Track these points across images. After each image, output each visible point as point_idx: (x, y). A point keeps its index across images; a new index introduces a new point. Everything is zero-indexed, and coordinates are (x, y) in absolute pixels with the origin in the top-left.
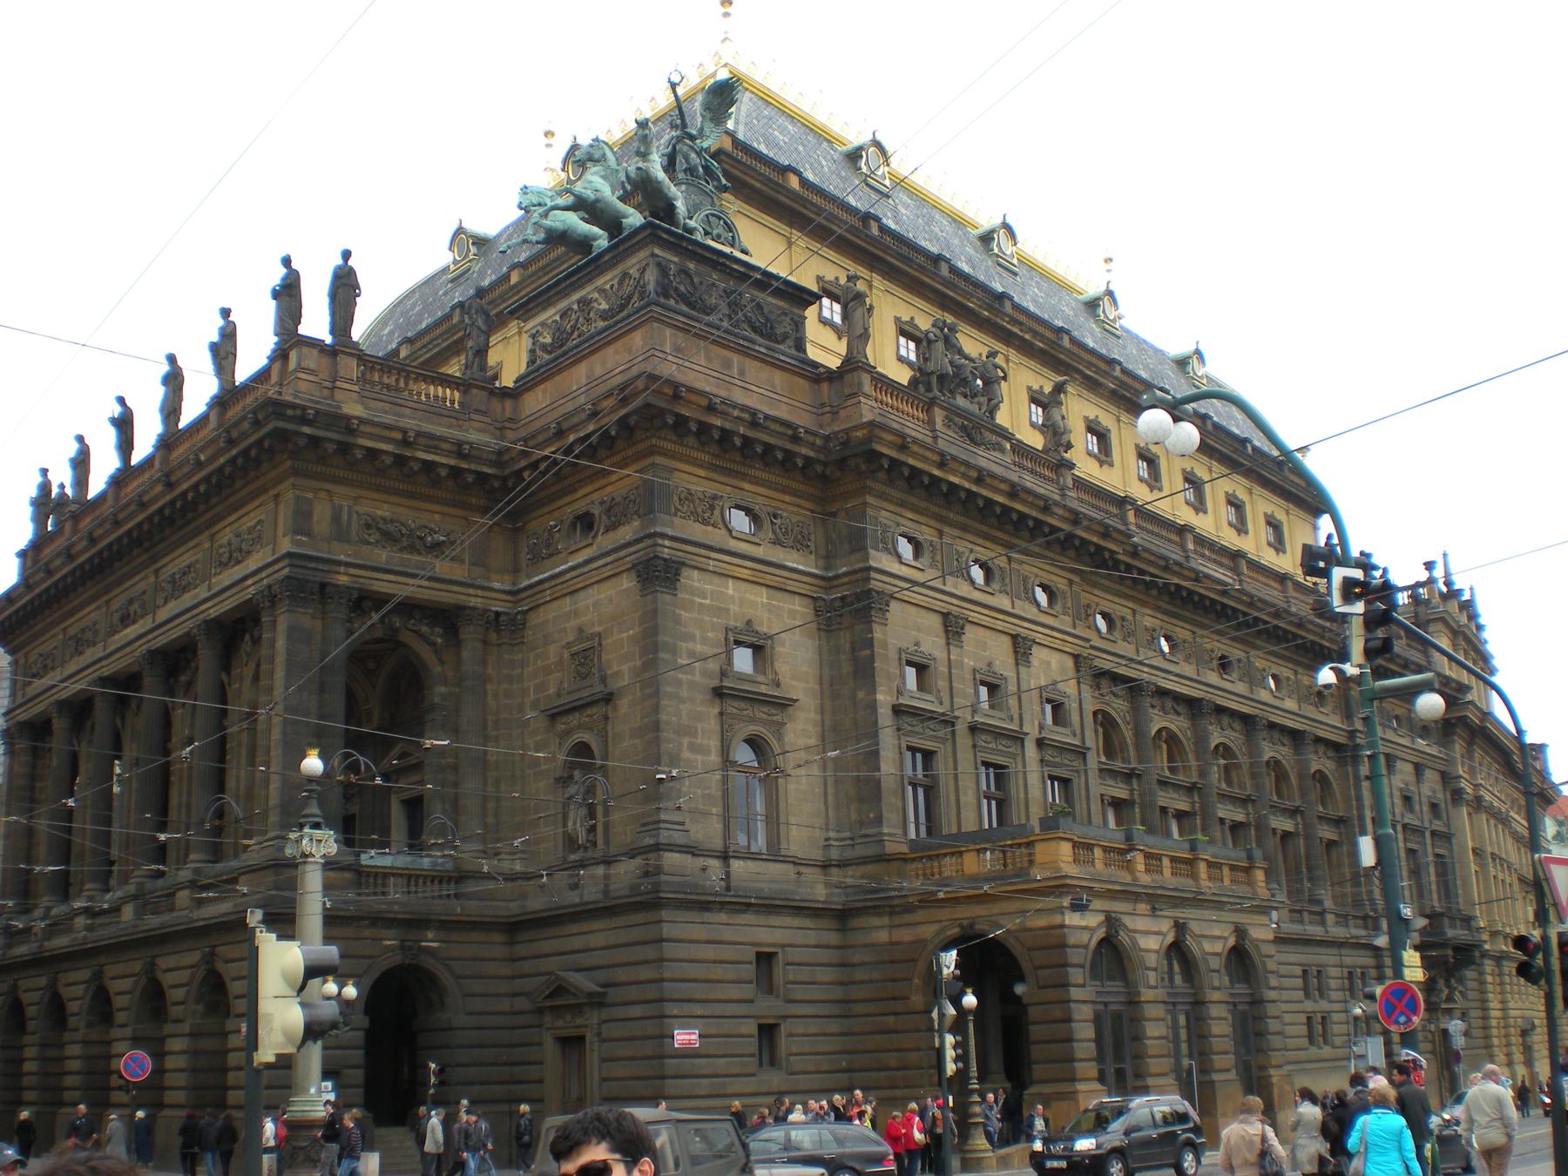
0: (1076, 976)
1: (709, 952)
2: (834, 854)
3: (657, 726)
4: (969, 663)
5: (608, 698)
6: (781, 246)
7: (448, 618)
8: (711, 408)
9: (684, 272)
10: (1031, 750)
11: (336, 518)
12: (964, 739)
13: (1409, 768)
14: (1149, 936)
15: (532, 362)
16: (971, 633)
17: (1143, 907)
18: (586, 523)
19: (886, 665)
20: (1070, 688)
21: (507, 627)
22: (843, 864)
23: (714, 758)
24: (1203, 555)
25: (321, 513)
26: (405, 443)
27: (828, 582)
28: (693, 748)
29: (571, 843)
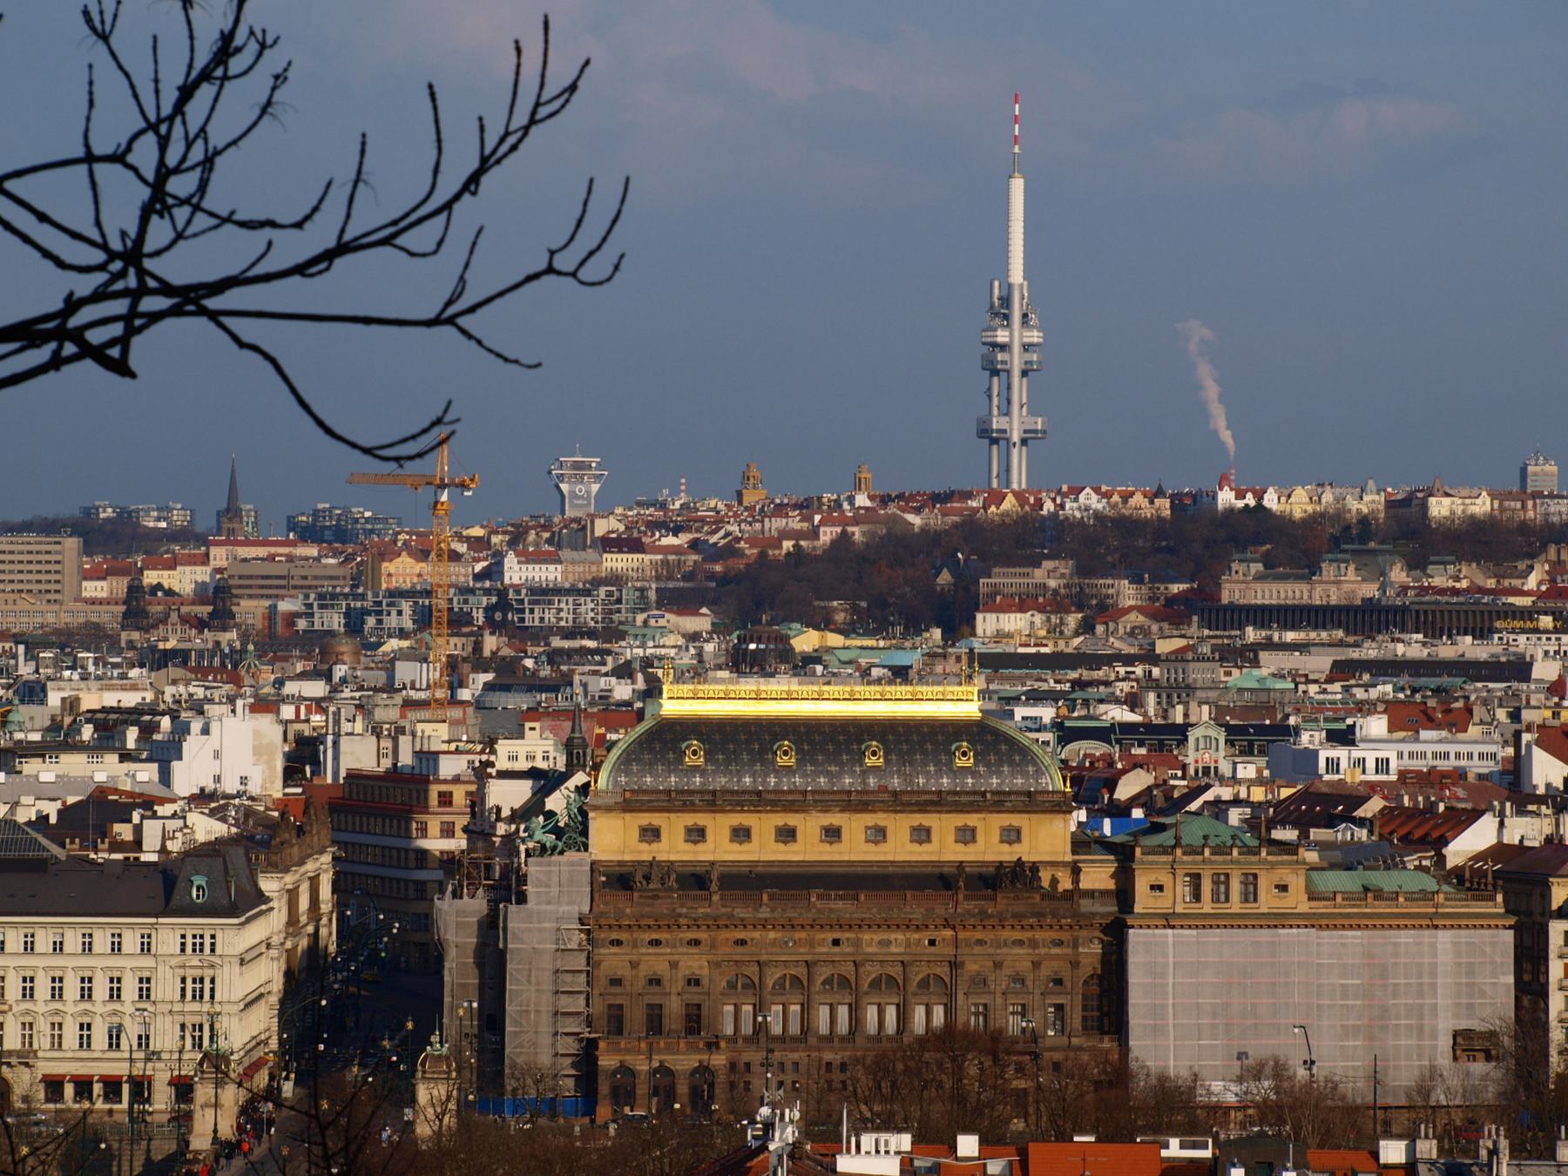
4: (642, 974)
6: (620, 822)
10: (674, 997)
14: (642, 1066)
20: (705, 972)
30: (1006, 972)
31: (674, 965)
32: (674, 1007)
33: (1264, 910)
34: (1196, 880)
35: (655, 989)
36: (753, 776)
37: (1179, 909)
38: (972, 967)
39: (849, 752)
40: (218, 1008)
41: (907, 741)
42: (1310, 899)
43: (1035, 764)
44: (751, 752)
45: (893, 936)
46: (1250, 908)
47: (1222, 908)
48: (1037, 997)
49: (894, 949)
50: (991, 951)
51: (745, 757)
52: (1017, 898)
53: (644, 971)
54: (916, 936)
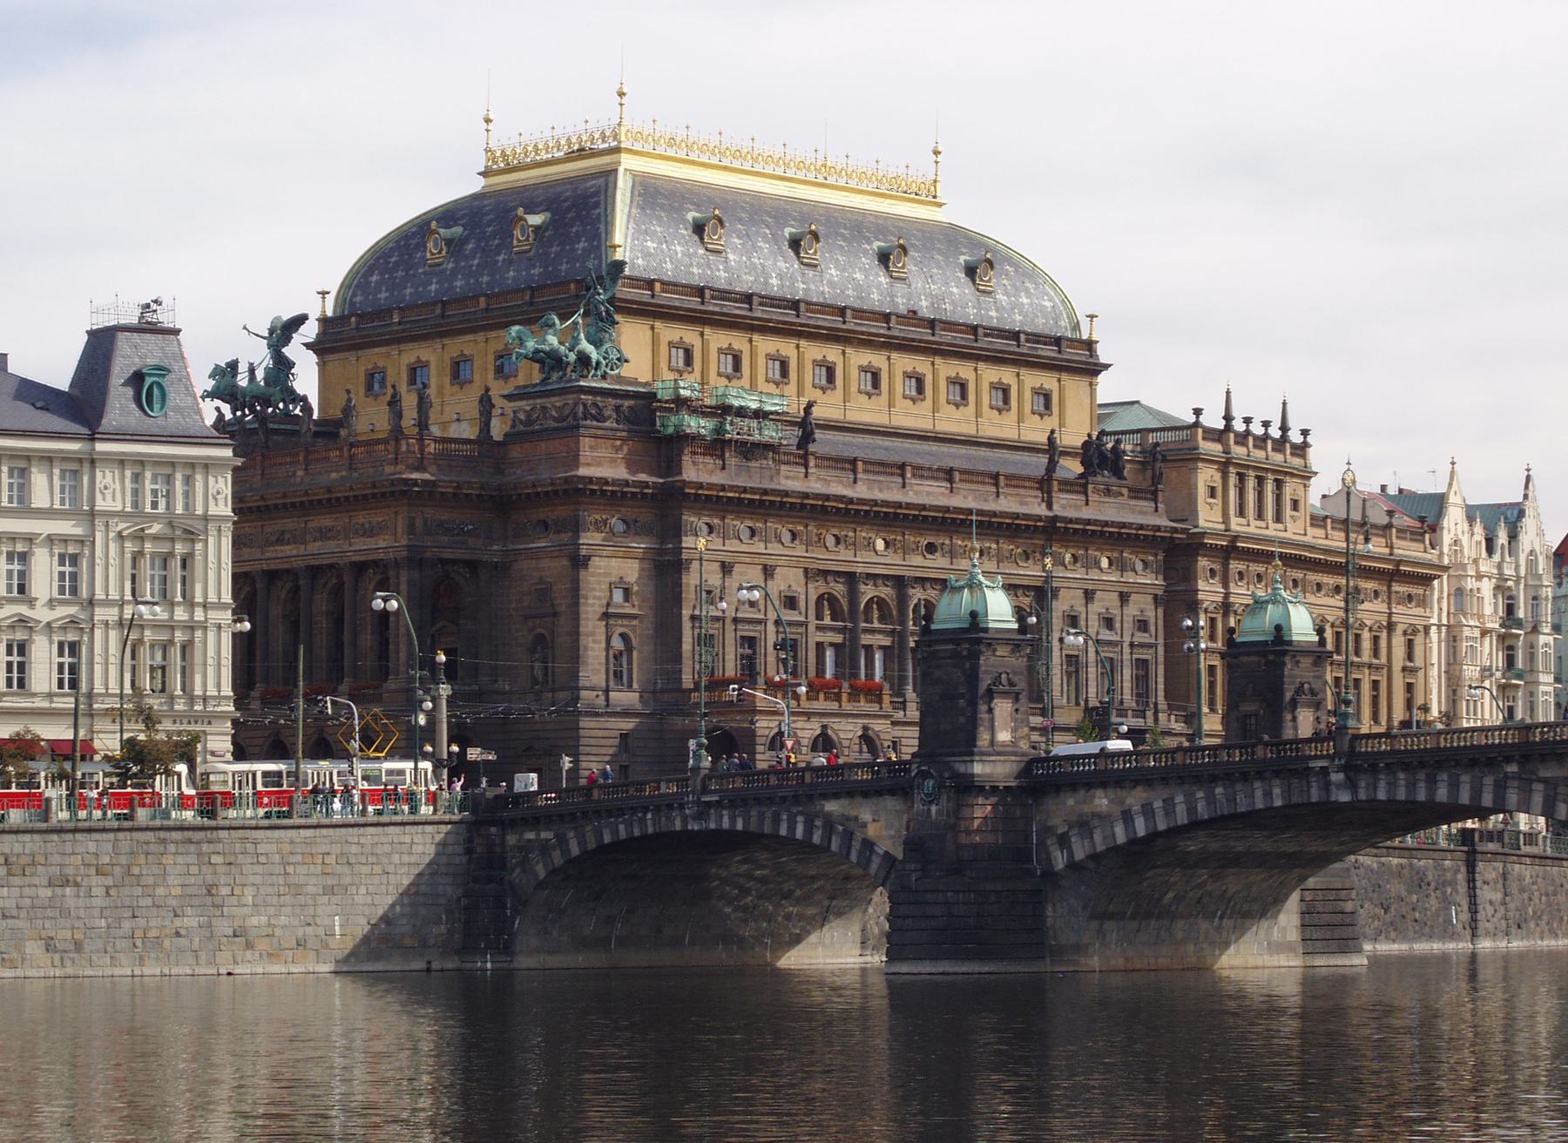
0: (760, 748)
1: (600, 733)
3: (578, 634)
5: (555, 615)
7: (473, 565)
8: (607, 483)
9: (595, 404)
11: (425, 524)
12: (730, 627)
13: (1115, 596)
15: (513, 426)
16: (737, 568)
18: (545, 525)
19: (689, 596)
21: (502, 569)
22: (662, 691)
23: (603, 645)
24: (922, 477)
25: (419, 523)
26: (458, 487)
27: (661, 552)
28: (594, 642)
29: (535, 681)
30: (1096, 607)
36: (780, 276)
40: (199, 615)
48: (1126, 650)
52: (1108, 492)
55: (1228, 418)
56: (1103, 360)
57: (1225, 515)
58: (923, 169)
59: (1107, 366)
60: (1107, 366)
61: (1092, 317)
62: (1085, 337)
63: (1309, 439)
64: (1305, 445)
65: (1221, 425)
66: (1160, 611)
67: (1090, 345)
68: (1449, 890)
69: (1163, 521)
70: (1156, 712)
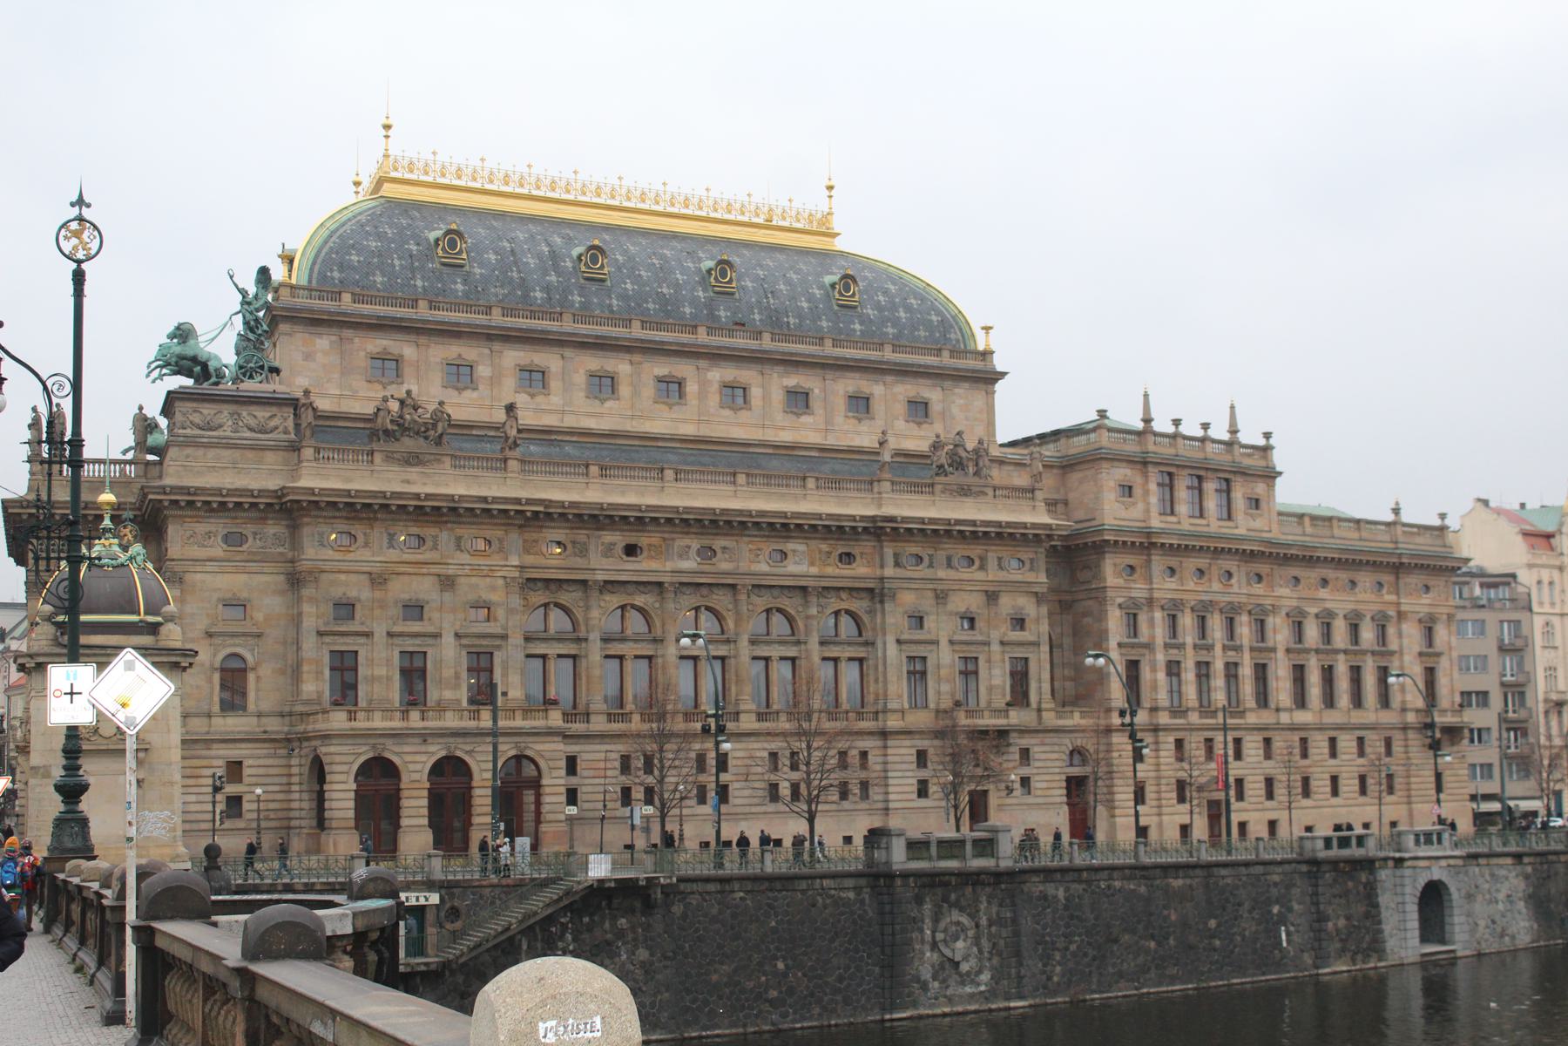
2: (287, 709)
10: (448, 639)
17: (417, 740)
31: (447, 583)
32: (447, 658)
33: (1241, 531)
34: (1169, 485)
35: (416, 627)
36: (547, 289)
37: (1156, 523)
38: (908, 599)
39: (684, 271)
41: (761, 266)
42: (1280, 523)
43: (939, 313)
44: (539, 256)
45: (790, 546)
46: (1226, 529)
47: (1199, 526)
48: (996, 647)
49: (792, 567)
50: (929, 573)
51: (532, 262)
53: (400, 589)
54: (824, 547)
55: (1147, 420)
56: (999, 369)
57: (1147, 511)
58: (815, 202)
59: (1003, 374)
60: (1003, 374)
61: (987, 329)
62: (981, 347)
63: (1272, 441)
64: (1266, 450)
65: (1140, 426)
66: (1044, 610)
67: (986, 354)
68: (1276, 909)
69: (1044, 518)
70: (1039, 710)
